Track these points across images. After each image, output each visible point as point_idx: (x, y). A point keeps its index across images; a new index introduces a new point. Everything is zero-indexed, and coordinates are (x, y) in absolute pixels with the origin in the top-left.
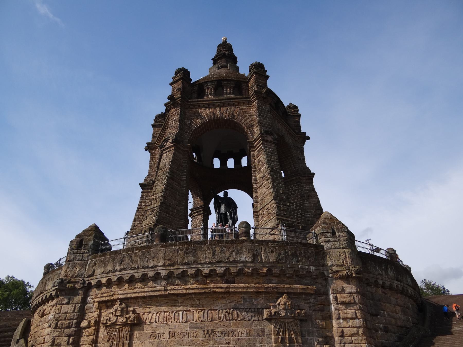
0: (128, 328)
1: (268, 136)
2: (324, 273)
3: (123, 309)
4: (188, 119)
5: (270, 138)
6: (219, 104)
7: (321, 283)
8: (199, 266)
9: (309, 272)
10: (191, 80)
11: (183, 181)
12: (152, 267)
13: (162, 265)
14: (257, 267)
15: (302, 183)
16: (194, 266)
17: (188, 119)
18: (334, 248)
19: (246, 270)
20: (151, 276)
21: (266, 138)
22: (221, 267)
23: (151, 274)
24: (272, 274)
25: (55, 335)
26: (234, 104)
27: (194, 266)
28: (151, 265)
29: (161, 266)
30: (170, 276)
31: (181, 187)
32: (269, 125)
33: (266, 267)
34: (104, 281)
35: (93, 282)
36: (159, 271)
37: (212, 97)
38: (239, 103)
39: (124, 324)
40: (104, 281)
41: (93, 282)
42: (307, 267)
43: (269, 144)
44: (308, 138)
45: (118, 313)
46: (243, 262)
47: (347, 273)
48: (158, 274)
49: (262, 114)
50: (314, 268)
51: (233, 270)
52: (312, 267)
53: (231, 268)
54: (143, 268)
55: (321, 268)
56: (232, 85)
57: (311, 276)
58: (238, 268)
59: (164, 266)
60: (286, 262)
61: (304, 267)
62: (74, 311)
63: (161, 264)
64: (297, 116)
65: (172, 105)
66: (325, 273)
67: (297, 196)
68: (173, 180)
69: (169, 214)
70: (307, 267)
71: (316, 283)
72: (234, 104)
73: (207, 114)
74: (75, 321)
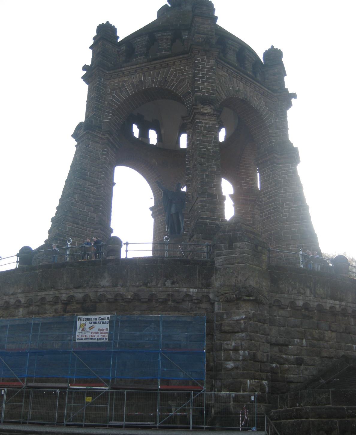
1: (206, 107)
2: (209, 297)
4: (109, 94)
6: (148, 68)
7: (206, 309)
8: (57, 292)
9: (187, 295)
10: (118, 37)
11: (101, 179)
12: (13, 294)
13: (21, 292)
14: (121, 293)
15: (278, 164)
16: (51, 292)
17: (109, 94)
18: (226, 265)
19: (108, 296)
20: (12, 304)
22: (79, 293)
23: (12, 301)
24: (140, 300)
26: (168, 64)
27: (51, 292)
28: (11, 292)
29: (20, 293)
30: (30, 303)
31: (97, 188)
32: (212, 90)
33: (132, 291)
36: (20, 299)
38: (174, 62)
42: (185, 290)
43: (207, 117)
44: (294, 96)
46: (103, 287)
47: (236, 295)
48: (19, 301)
49: (202, 74)
50: (196, 290)
51: (92, 295)
52: (192, 290)
53: (90, 294)
54: (5, 295)
55: (205, 290)
56: (169, 37)
57: (192, 300)
58: (99, 294)
59: (23, 292)
60: (157, 284)
61: (181, 290)
63: (19, 291)
66: (211, 296)
67: (271, 184)
68: (84, 179)
69: (78, 224)
70: (185, 290)
71: (199, 308)
72: (168, 64)
73: (133, 84)
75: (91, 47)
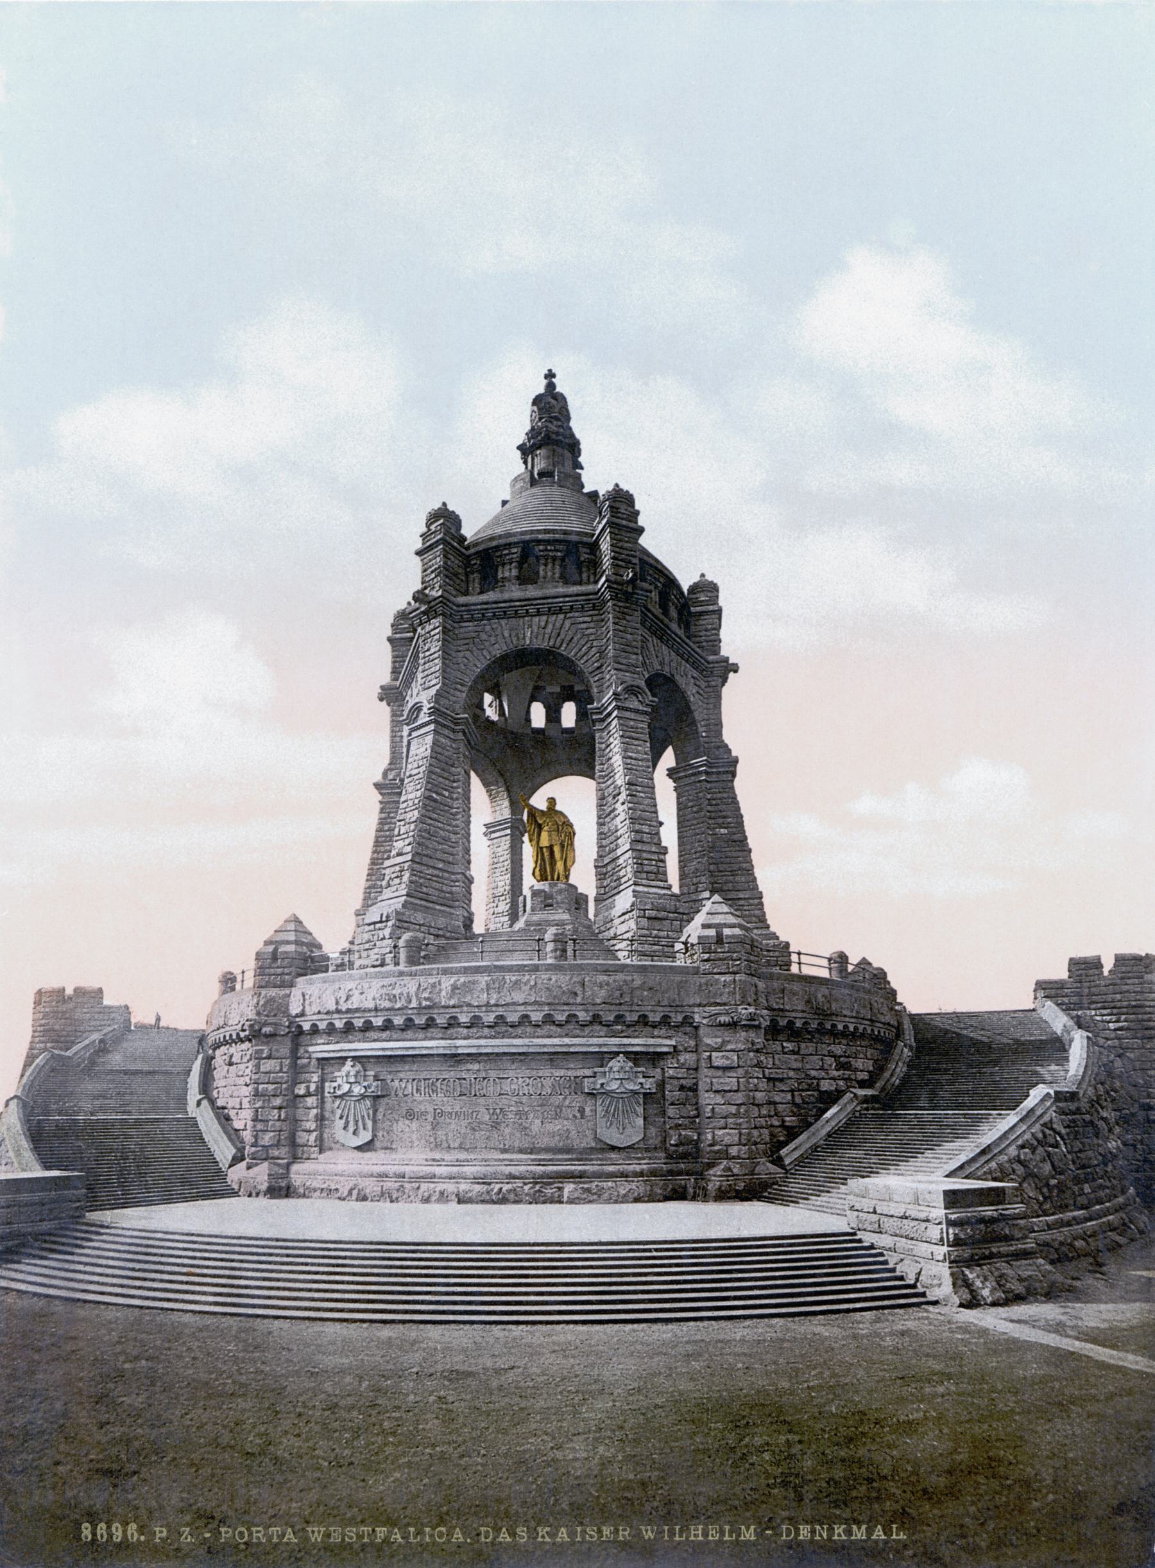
0: (368, 1102)
3: (358, 1072)
5: (634, 704)
21: (627, 704)
25: (257, 1106)
34: (322, 1026)
35: (306, 1027)
37: (515, 592)
39: (363, 1097)
40: (322, 1026)
41: (306, 1027)
45: (352, 1080)
62: (281, 1071)
64: (714, 612)
65: (424, 613)
74: (284, 1086)
75: (419, 553)
